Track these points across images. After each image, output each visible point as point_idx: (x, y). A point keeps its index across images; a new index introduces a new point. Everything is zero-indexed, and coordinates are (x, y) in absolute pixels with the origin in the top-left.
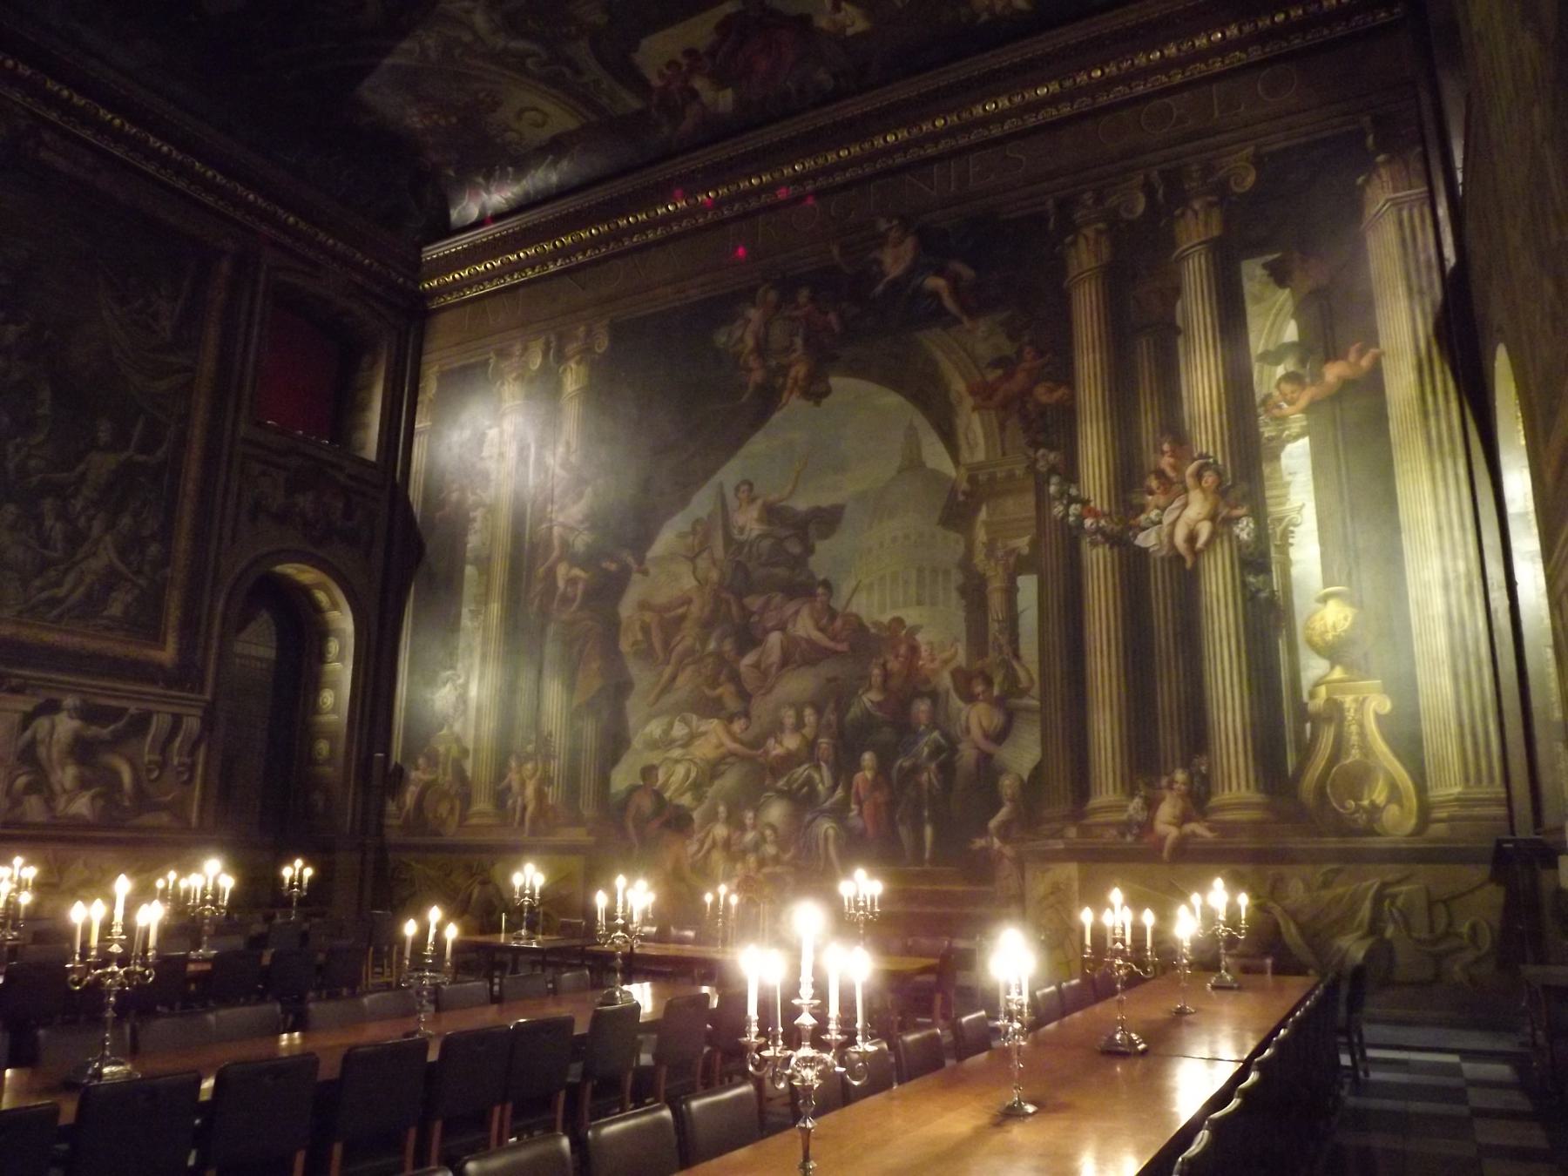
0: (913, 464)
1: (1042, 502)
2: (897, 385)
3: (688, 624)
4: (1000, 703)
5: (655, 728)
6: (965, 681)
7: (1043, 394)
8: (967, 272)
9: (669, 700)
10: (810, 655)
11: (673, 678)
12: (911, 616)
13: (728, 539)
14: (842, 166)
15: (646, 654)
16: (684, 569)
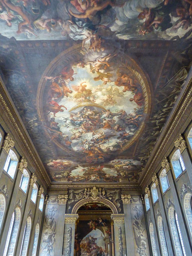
0: (102, 236)
1: (109, 239)
2: (100, 230)
3: (86, 246)
4: (107, 253)
5: (83, 253)
6: (105, 251)
7: (110, 233)
8: (105, 223)
9: (84, 252)
10: (95, 249)
11: (84, 250)
12: (102, 247)
13: (89, 239)
14: (97, 213)
15: (82, 247)
16: (86, 241)
